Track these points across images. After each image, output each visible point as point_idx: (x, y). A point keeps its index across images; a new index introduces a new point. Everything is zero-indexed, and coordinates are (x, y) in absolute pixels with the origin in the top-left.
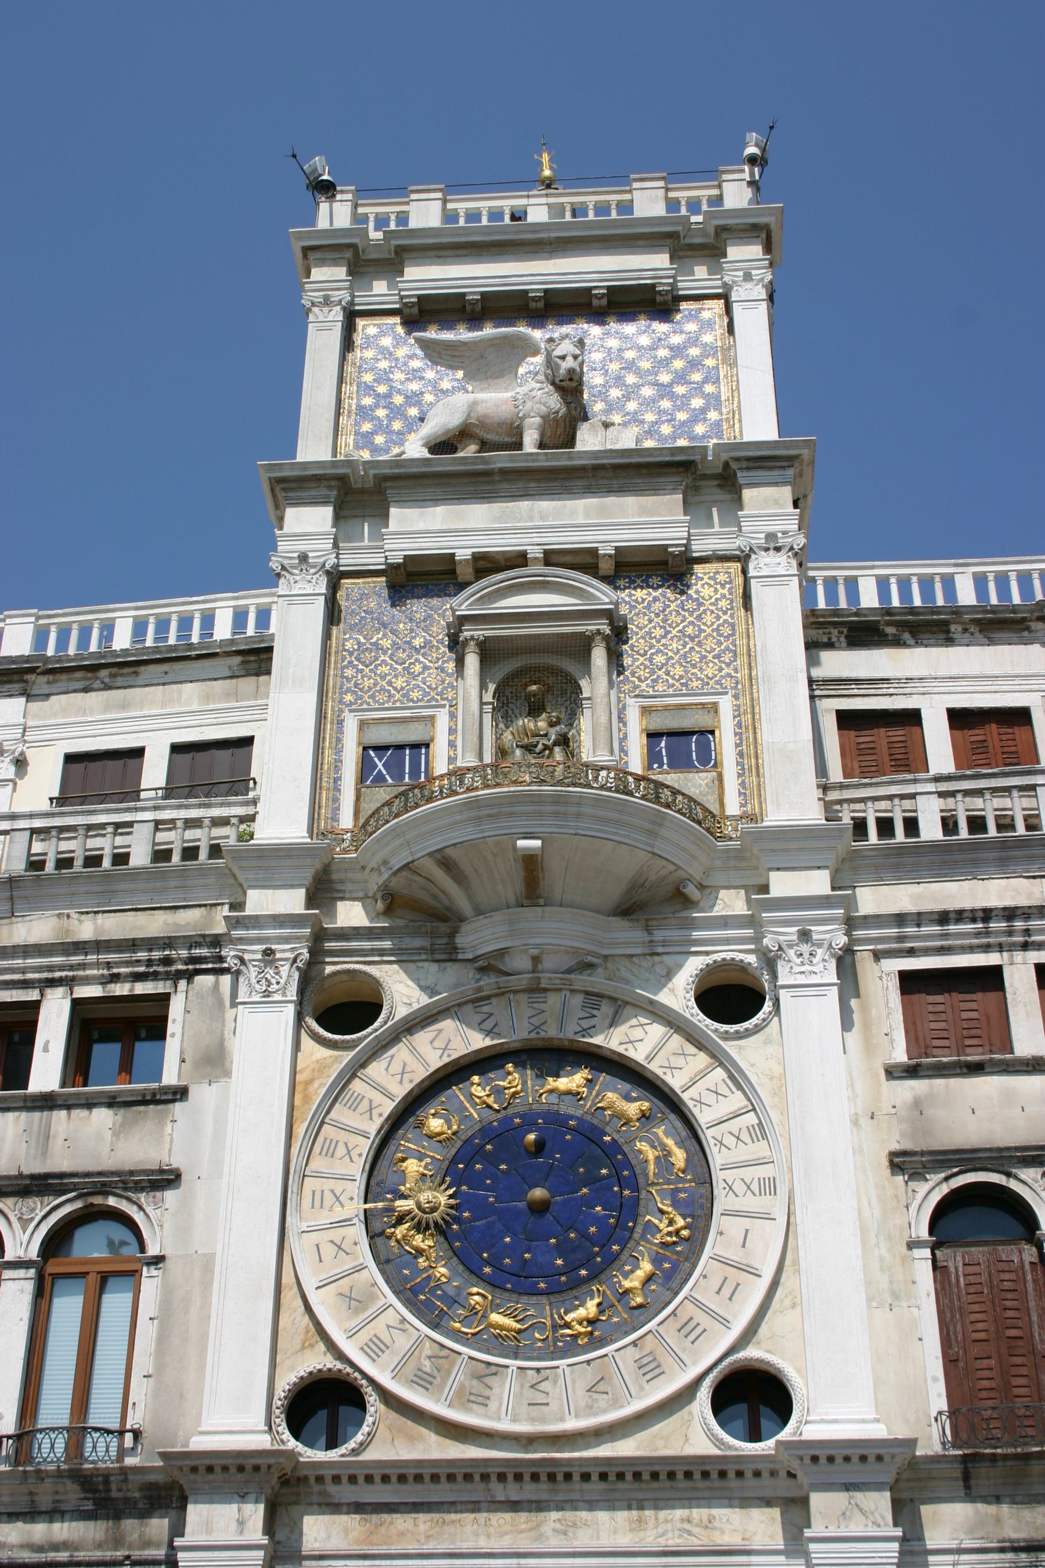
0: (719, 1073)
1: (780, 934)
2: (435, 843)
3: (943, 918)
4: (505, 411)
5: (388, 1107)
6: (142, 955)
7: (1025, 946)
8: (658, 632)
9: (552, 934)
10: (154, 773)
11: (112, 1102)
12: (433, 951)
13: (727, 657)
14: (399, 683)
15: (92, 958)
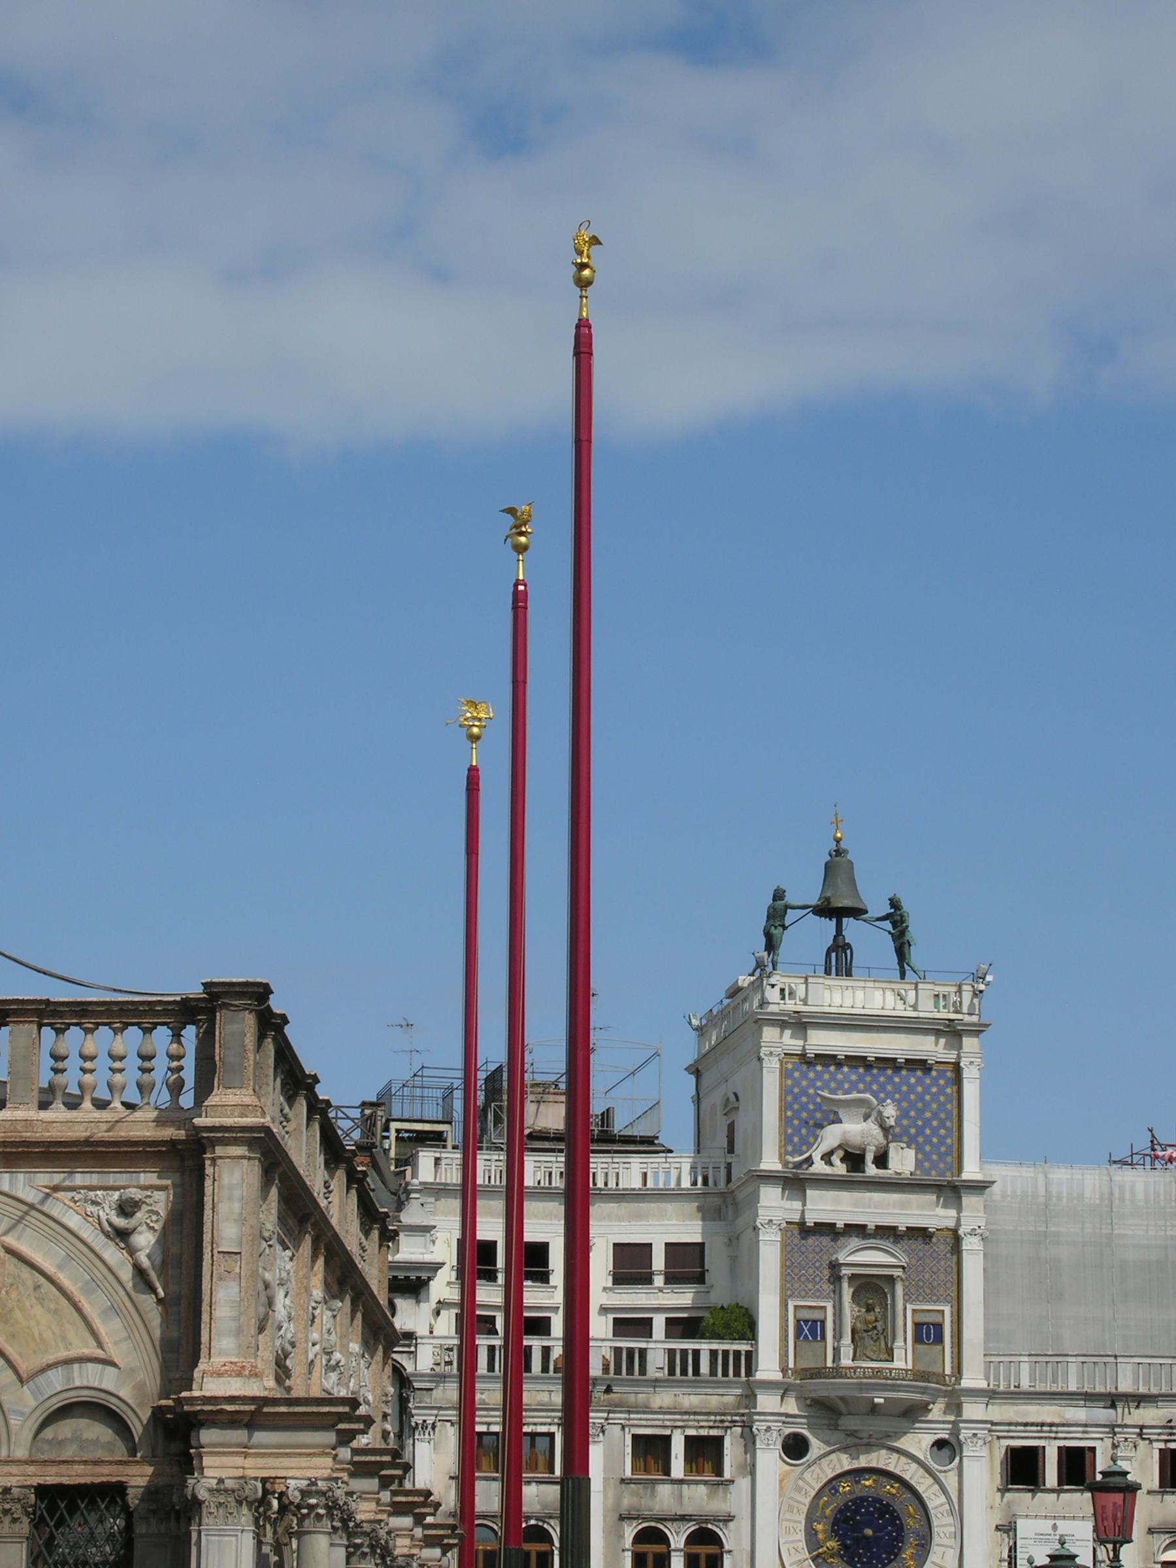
0: (936, 1487)
1: (964, 1434)
2: (841, 1393)
3: (1026, 1425)
4: (856, 1140)
5: (813, 1493)
6: (712, 1418)
7: (1055, 1438)
8: (920, 1268)
9: (878, 1425)
10: (658, 1262)
11: (705, 1483)
12: (829, 1425)
13: (949, 1285)
14: (810, 1286)
15: (692, 1417)
